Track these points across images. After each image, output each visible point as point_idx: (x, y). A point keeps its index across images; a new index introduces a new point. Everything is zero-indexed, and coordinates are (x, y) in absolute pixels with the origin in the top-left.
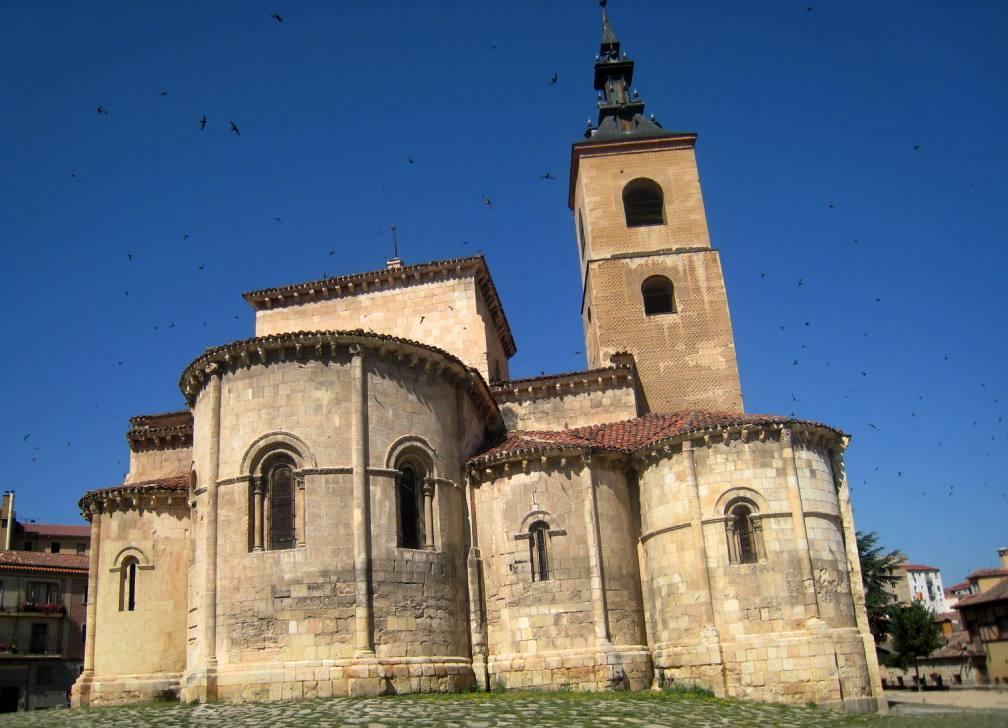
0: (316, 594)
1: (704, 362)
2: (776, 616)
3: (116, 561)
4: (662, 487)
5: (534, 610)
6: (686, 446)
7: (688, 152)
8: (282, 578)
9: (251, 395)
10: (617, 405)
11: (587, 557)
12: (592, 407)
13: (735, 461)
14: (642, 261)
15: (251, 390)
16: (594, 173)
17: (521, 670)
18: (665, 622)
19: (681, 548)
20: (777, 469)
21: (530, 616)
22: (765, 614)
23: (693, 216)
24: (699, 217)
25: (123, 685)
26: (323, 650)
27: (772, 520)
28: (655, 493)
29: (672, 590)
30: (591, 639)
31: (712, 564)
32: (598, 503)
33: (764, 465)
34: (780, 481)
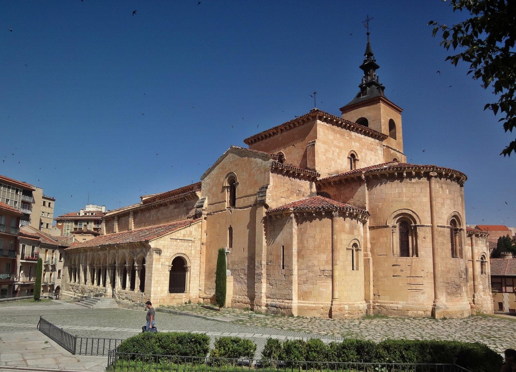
6: (474, 236)
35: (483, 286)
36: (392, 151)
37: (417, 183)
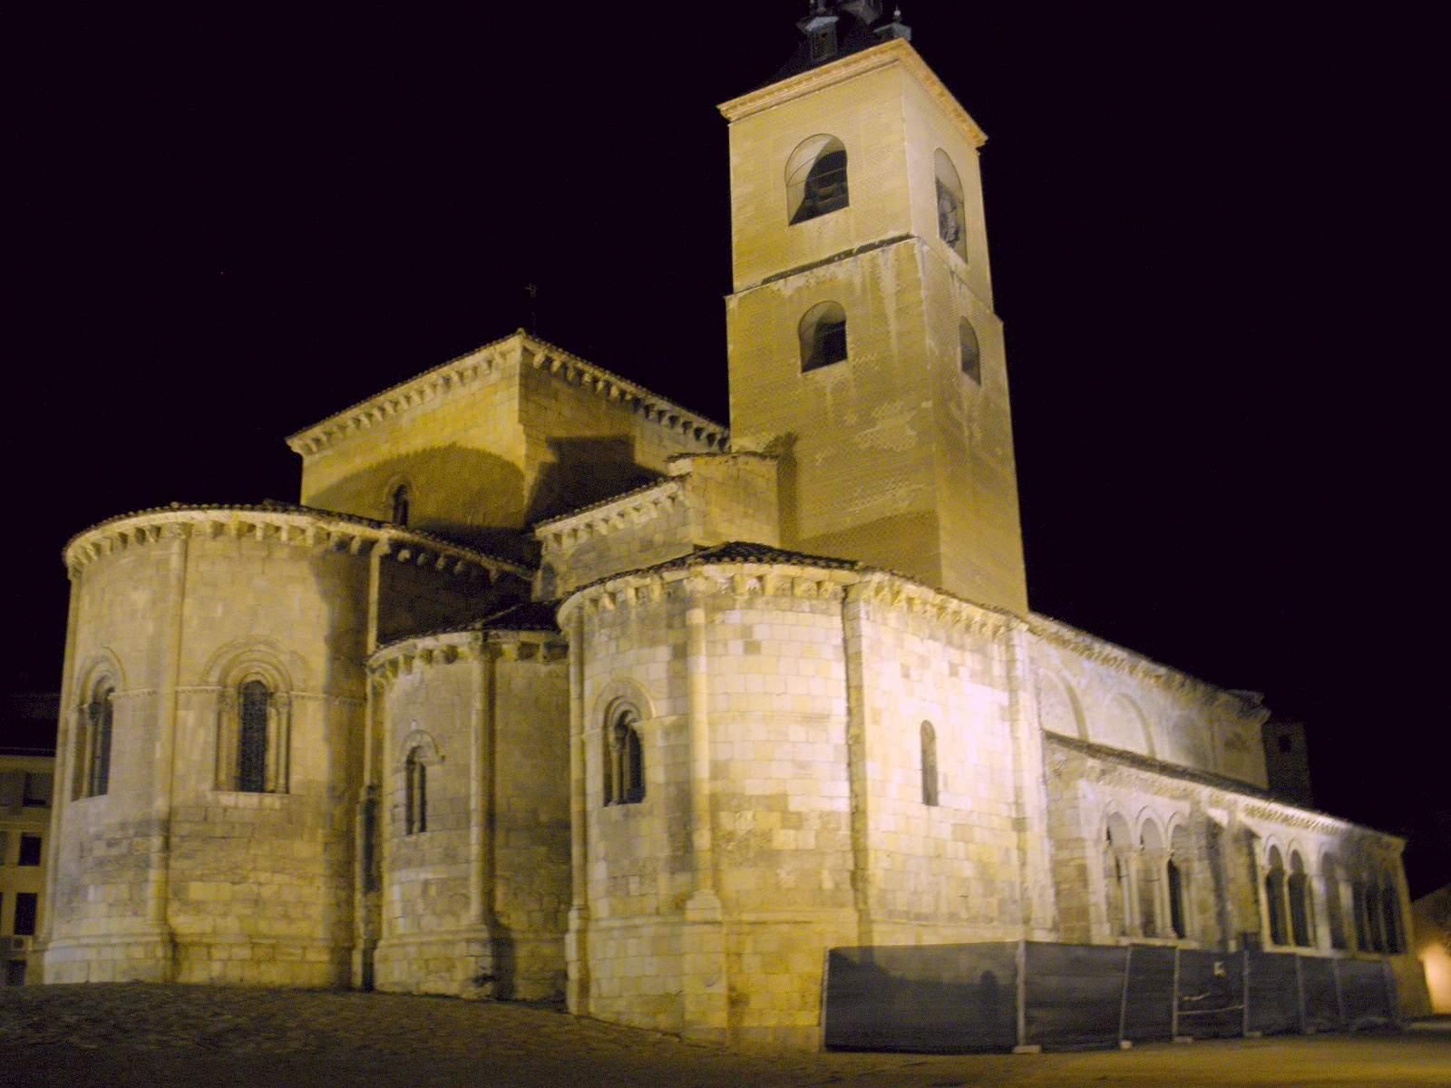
0: (114, 852)
11: (468, 798)
12: (641, 552)
32: (498, 712)
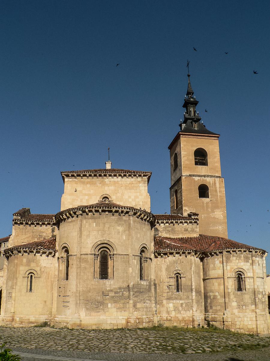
0: (117, 295)
1: (217, 216)
2: (247, 308)
3: (25, 274)
4: (214, 264)
5: (174, 301)
7: (217, 140)
8: (106, 289)
9: (95, 225)
10: (193, 231)
11: (192, 285)
13: (239, 260)
14: (199, 178)
15: (95, 223)
16: (185, 143)
17: (170, 320)
18: (211, 307)
19: (219, 285)
20: (250, 263)
21: (173, 303)
22: (244, 307)
23: (216, 164)
24: (218, 165)
25: (29, 319)
26: (119, 313)
27: (248, 279)
28: (211, 266)
29: (215, 297)
30: (191, 311)
31: (230, 291)
33: (247, 262)
34: (251, 267)
35: (237, 303)
36: (197, 178)
37: (72, 222)
